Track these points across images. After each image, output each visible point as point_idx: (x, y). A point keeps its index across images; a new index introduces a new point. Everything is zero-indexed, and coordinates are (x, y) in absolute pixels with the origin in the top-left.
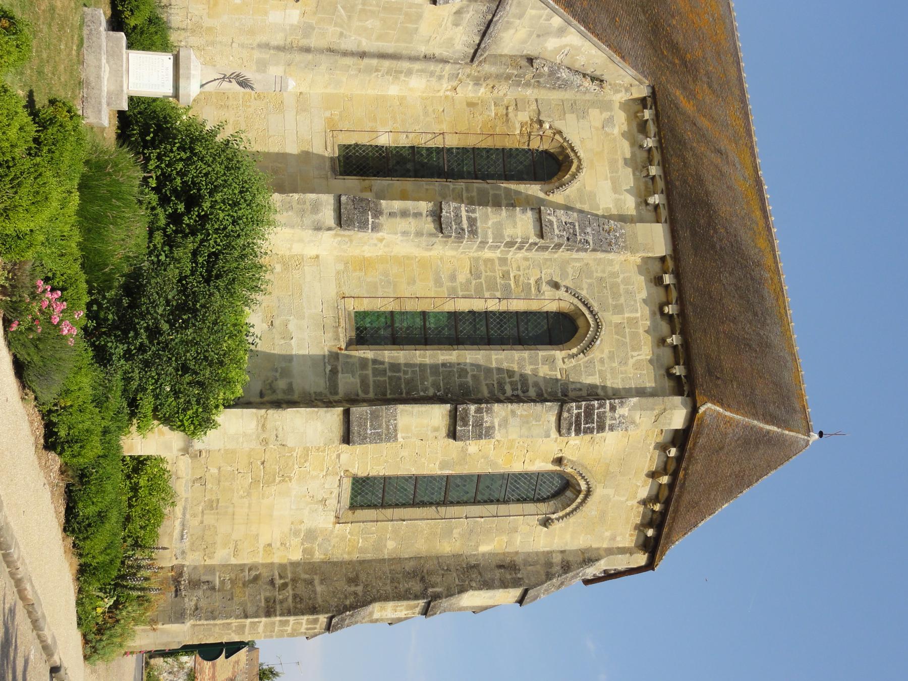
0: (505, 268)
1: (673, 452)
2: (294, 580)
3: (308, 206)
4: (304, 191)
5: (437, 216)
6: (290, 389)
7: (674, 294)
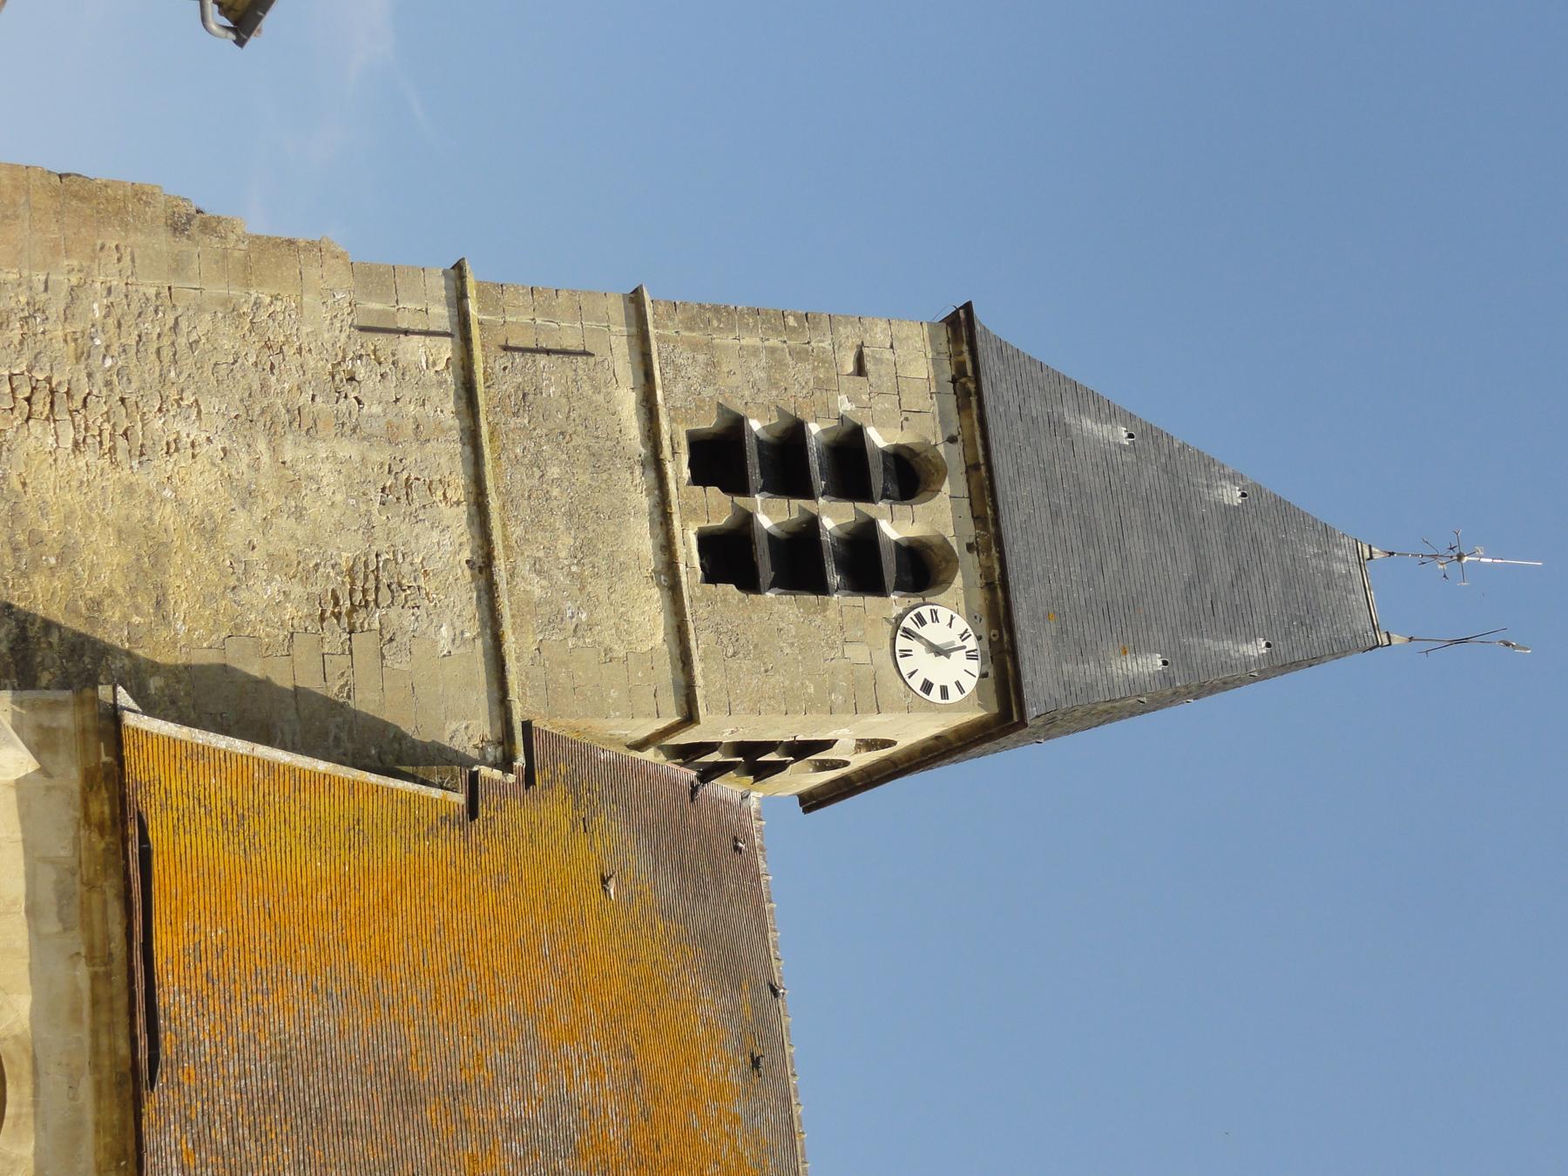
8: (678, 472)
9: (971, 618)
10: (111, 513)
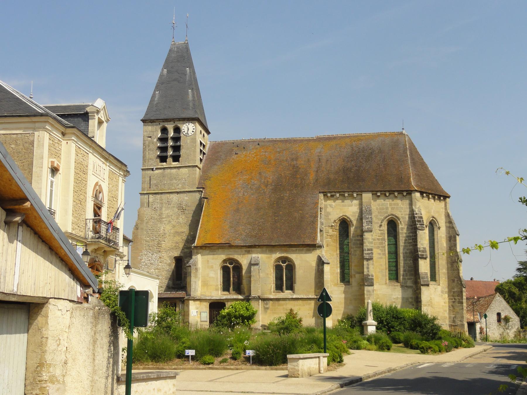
0: (376, 239)
1: (425, 195)
2: (453, 296)
3: (368, 293)
5: (368, 260)
6: (411, 298)
7: (383, 192)
9: (184, 124)
10: (172, 238)
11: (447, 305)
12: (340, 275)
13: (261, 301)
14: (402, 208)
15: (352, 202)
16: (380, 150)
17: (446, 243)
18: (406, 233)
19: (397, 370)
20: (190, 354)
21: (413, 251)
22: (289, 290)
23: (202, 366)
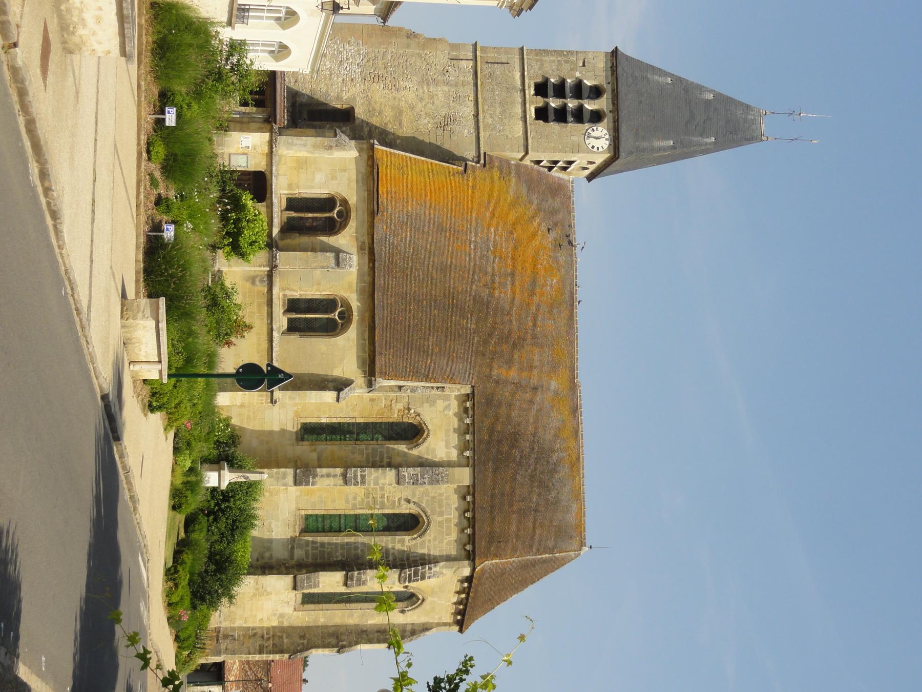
0: (382, 492)
1: (466, 585)
2: (273, 636)
3: (281, 476)
4: (278, 467)
5: (344, 476)
6: (271, 557)
8: (530, 92)
9: (608, 130)
11: (257, 625)
12: (316, 423)
13: (268, 271)
14: (442, 542)
15: (453, 447)
16: (552, 503)
17: (374, 625)
18: (394, 549)
19: (135, 515)
20: (167, 116)
21: (360, 561)
22: (288, 325)
23: (144, 138)
